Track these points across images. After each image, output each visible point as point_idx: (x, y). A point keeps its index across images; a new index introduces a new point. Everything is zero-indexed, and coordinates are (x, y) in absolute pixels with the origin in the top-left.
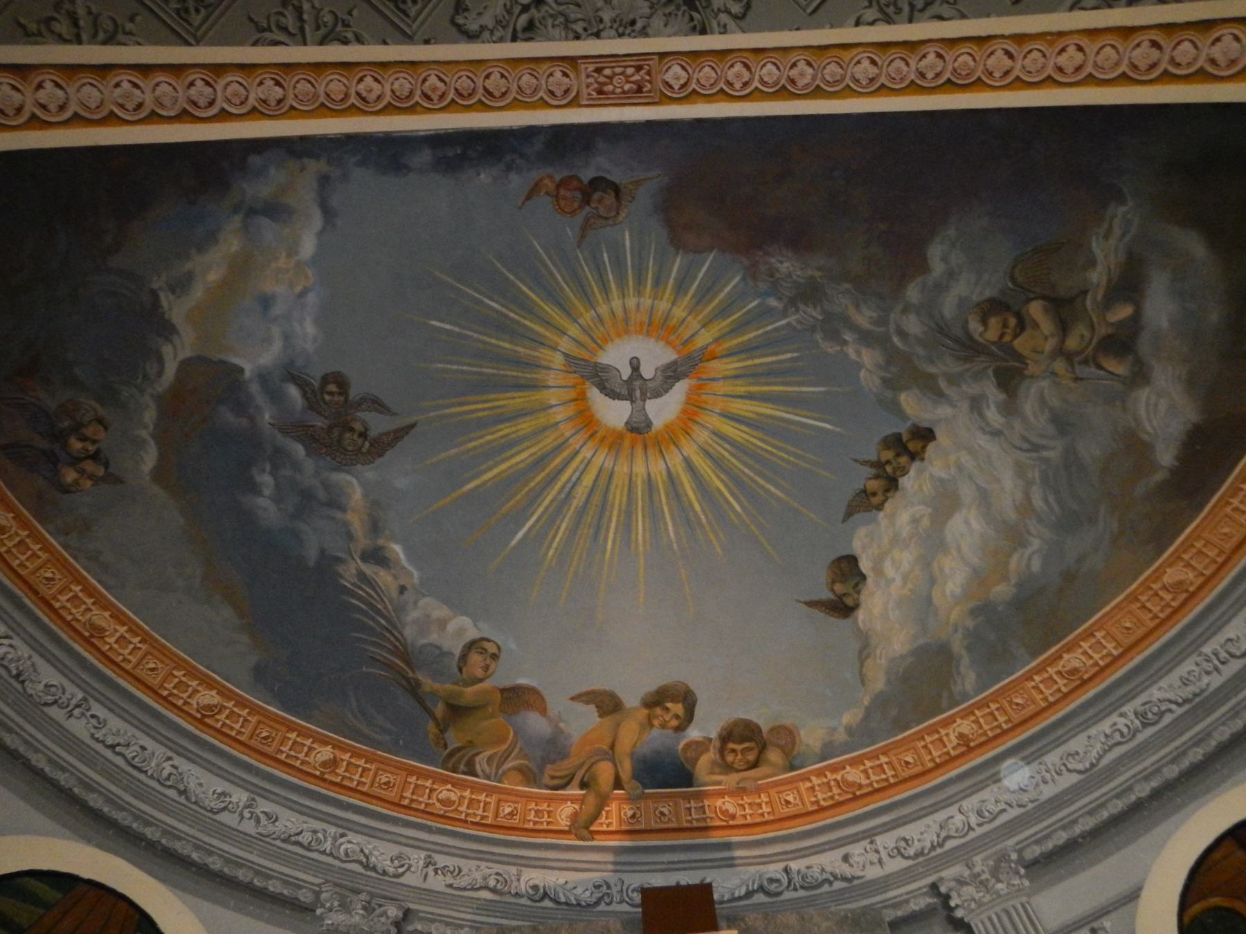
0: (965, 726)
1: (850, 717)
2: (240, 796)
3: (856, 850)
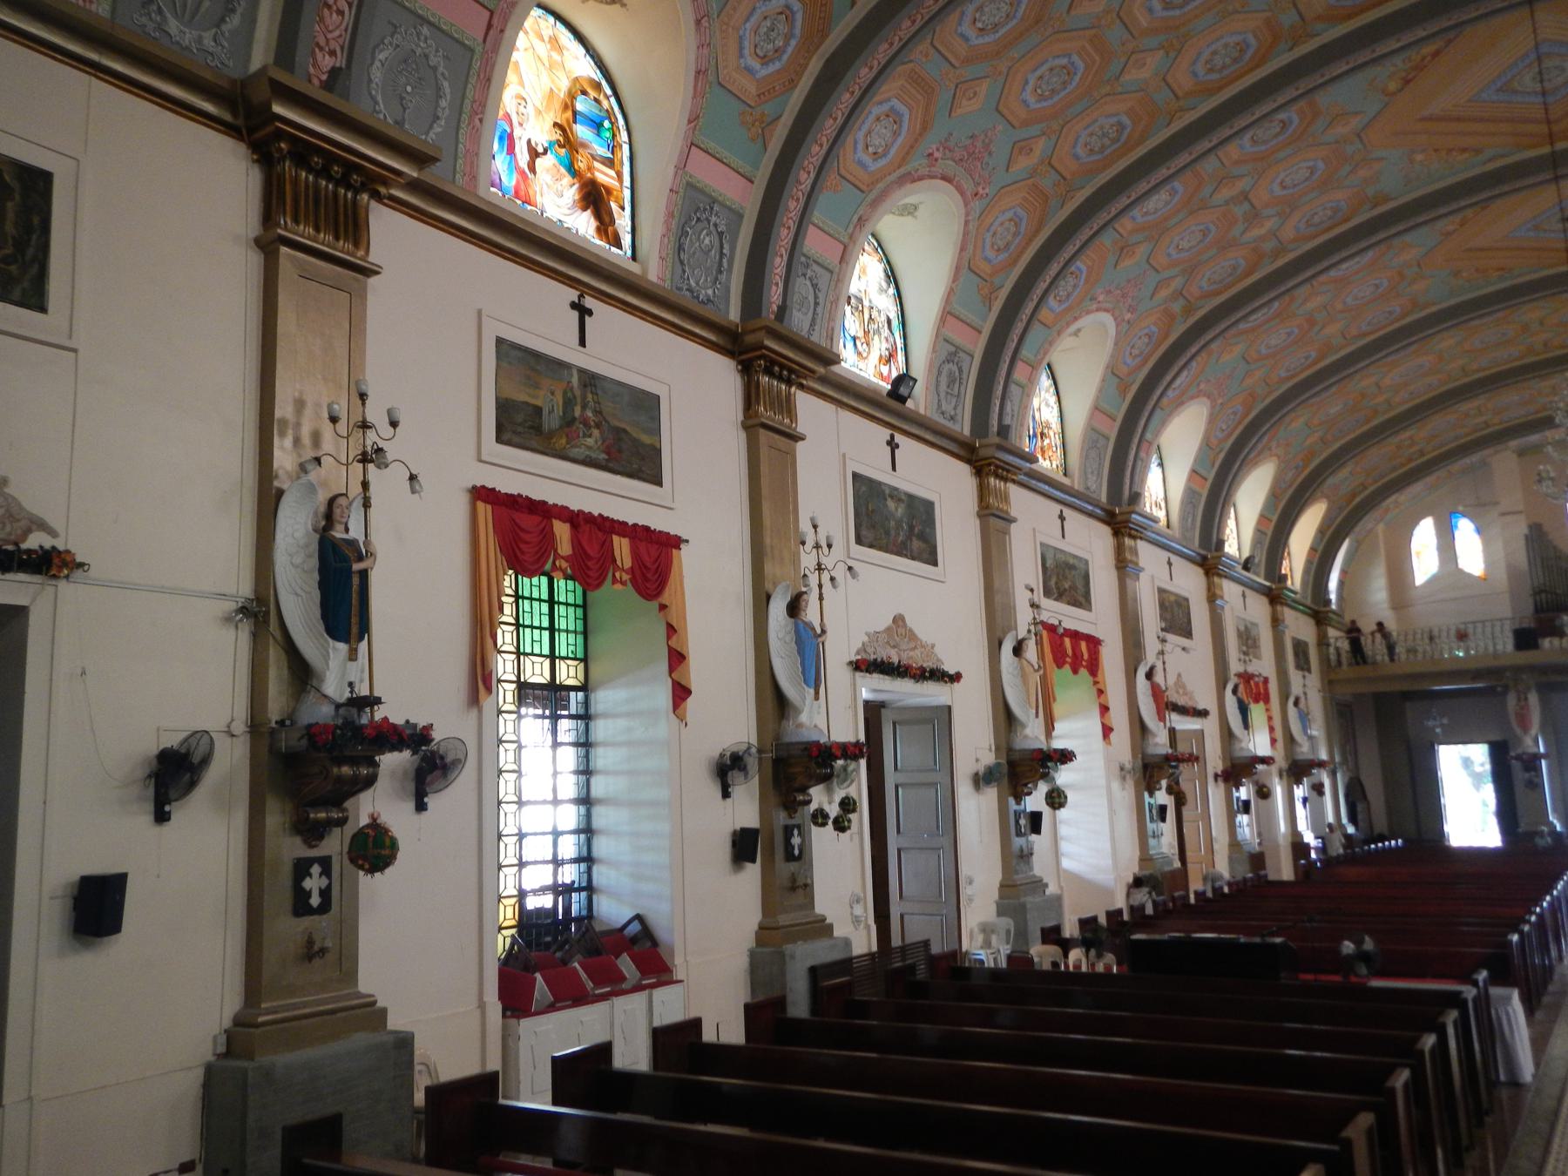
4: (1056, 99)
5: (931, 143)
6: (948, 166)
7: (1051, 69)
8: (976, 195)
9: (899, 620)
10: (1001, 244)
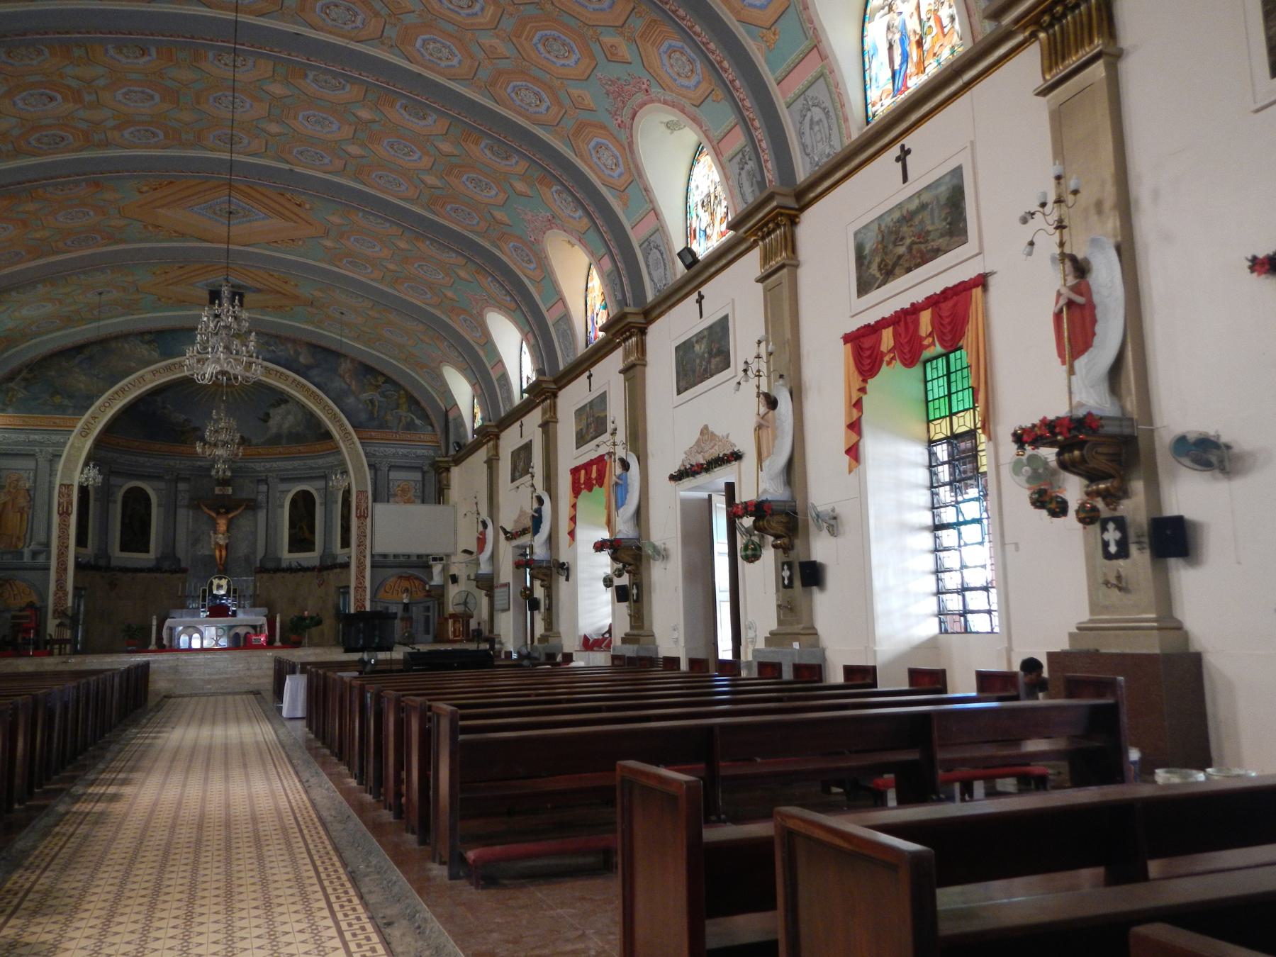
0: (281, 450)
1: (262, 440)
2: (147, 459)
3: (257, 464)
4: (568, 40)
5: (612, 124)
6: (627, 112)
7: (549, 52)
8: (647, 91)
9: (705, 430)
10: (688, 67)
